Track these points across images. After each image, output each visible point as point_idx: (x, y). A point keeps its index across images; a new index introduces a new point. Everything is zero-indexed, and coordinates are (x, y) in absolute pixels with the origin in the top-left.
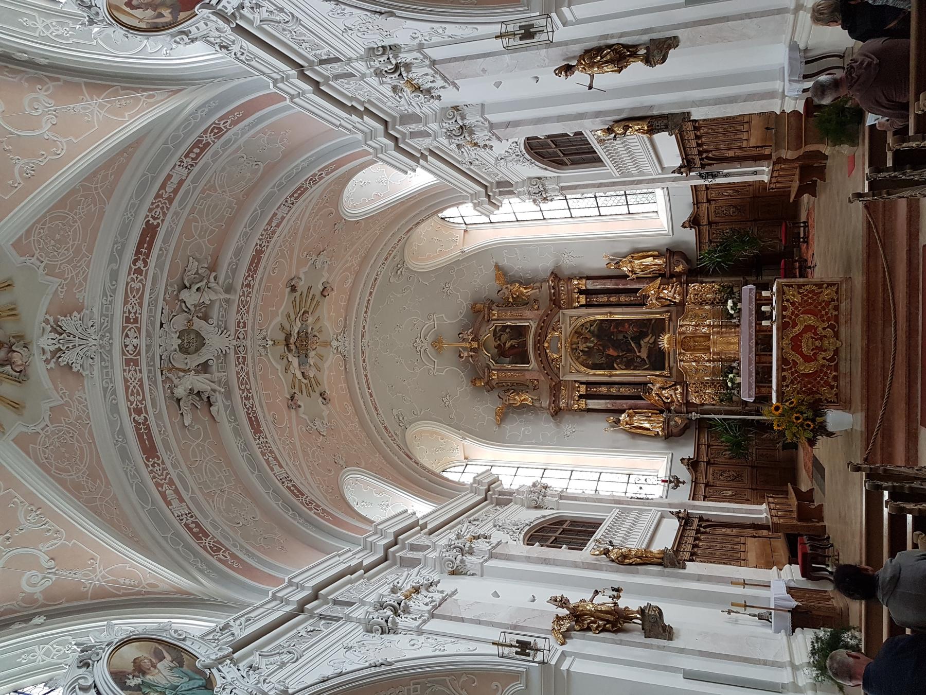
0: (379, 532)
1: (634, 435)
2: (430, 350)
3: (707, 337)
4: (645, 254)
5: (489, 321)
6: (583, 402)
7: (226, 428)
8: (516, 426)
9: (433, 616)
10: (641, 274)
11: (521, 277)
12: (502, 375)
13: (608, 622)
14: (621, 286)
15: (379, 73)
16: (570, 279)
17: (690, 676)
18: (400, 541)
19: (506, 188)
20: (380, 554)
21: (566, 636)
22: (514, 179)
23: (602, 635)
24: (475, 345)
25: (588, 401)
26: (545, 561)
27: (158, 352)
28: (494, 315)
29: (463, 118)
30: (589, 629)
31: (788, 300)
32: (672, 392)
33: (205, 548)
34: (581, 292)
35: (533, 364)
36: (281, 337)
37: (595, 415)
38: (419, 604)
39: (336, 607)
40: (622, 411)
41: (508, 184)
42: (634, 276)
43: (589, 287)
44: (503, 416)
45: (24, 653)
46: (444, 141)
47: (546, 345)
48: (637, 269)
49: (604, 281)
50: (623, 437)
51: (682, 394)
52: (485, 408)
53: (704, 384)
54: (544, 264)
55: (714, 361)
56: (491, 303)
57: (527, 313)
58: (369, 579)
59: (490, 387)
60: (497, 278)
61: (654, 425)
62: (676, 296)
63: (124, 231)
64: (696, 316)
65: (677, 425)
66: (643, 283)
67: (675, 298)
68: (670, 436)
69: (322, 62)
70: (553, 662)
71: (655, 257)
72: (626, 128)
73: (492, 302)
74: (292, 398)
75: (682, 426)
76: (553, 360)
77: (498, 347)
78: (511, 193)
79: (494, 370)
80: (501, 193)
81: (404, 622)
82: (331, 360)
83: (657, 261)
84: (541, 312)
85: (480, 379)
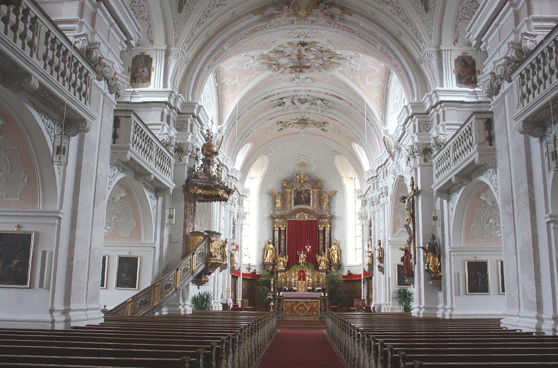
1: (264, 250)
2: (300, 161)
3: (304, 279)
6: (278, 229)
7: (272, 111)
10: (331, 254)
14: (326, 245)
15: (382, 188)
16: (330, 224)
19: (364, 203)
22: (367, 207)
26: (230, 230)
27: (299, 95)
29: (376, 204)
34: (324, 228)
35: (294, 208)
36: (305, 118)
41: (366, 204)
46: (371, 196)
50: (263, 246)
53: (286, 278)
54: (337, 212)
56: (321, 188)
57: (316, 205)
60: (331, 192)
61: (268, 259)
63: (340, 93)
64: (313, 276)
68: (264, 265)
69: (386, 170)
71: (338, 259)
72: (370, 257)
73: (321, 189)
74: (281, 122)
77: (301, 192)
78: (362, 206)
80: (362, 201)
82: (295, 130)
83: (336, 260)
84: (316, 211)
85: (287, 184)
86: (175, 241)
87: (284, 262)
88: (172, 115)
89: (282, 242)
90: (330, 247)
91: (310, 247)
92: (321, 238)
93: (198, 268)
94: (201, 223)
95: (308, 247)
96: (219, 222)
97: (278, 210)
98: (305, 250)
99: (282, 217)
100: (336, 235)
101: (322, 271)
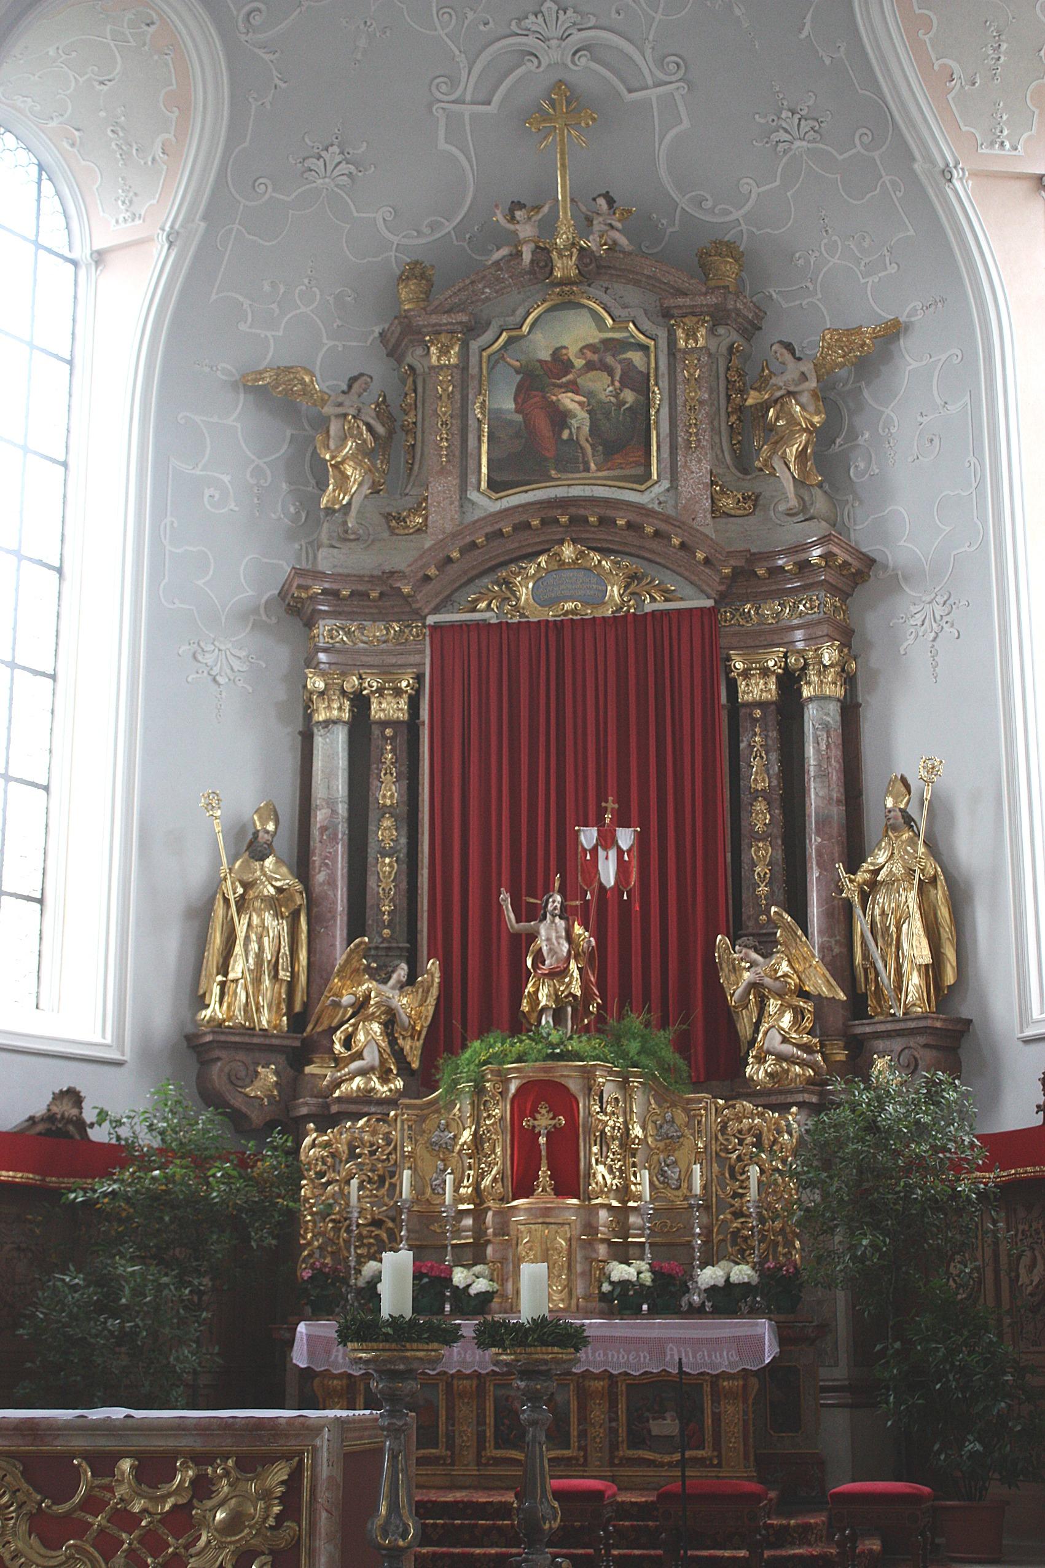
1: (200, 916)
3: (570, 1181)
4: (946, 932)
5: (667, 314)
6: (338, 710)
8: (237, 454)
11: (853, 435)
12: (444, 385)
14: (814, 842)
16: (847, 637)
24: (564, 267)
25: (340, 736)
28: (691, 334)
31: (202, 1488)
32: (371, 1057)
34: (789, 682)
35: (485, 503)
37: (290, 763)
40: (302, 868)
42: (851, 892)
43: (812, 712)
44: (278, 395)
47: (568, 552)
48: (882, 900)
49: (835, 776)
51: (366, 1098)
52: (320, 332)
53: (384, 1179)
54: (905, 520)
55: (478, 1214)
57: (698, 470)
59: (400, 339)
62: (770, 1065)
64: (670, 1142)
65: (235, 1081)
66: (828, 930)
67: (761, 1060)
68: (202, 1054)
71: (934, 971)
73: (751, 329)
75: (237, 1102)
76: (507, 583)
79: (465, 346)
83: (914, 981)
87: (390, 1021)
89: (386, 832)
90: (854, 853)
91: (625, 838)
92: (760, 772)
95: (607, 840)
97: (345, 537)
98: (574, 869)
99: (373, 597)
100: (913, 742)
101: (775, 1098)
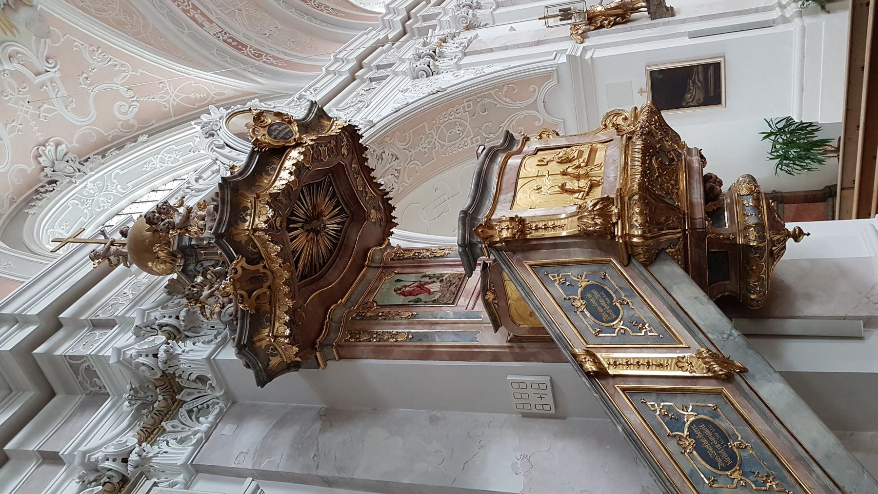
0: (392, 10)
9: (465, 54)
13: (618, 16)
17: (693, 35)
18: (412, 15)
20: (401, 28)
21: (584, 36)
23: (613, 28)
30: (602, 26)
33: (248, 55)
38: (451, 48)
39: (380, 71)
45: (145, 164)
58: (399, 48)
70: (578, 54)
81: (441, 64)
86: (549, 399)
88: (33, 447)
93: (692, 326)
94: (527, 107)
96: (518, 46)
